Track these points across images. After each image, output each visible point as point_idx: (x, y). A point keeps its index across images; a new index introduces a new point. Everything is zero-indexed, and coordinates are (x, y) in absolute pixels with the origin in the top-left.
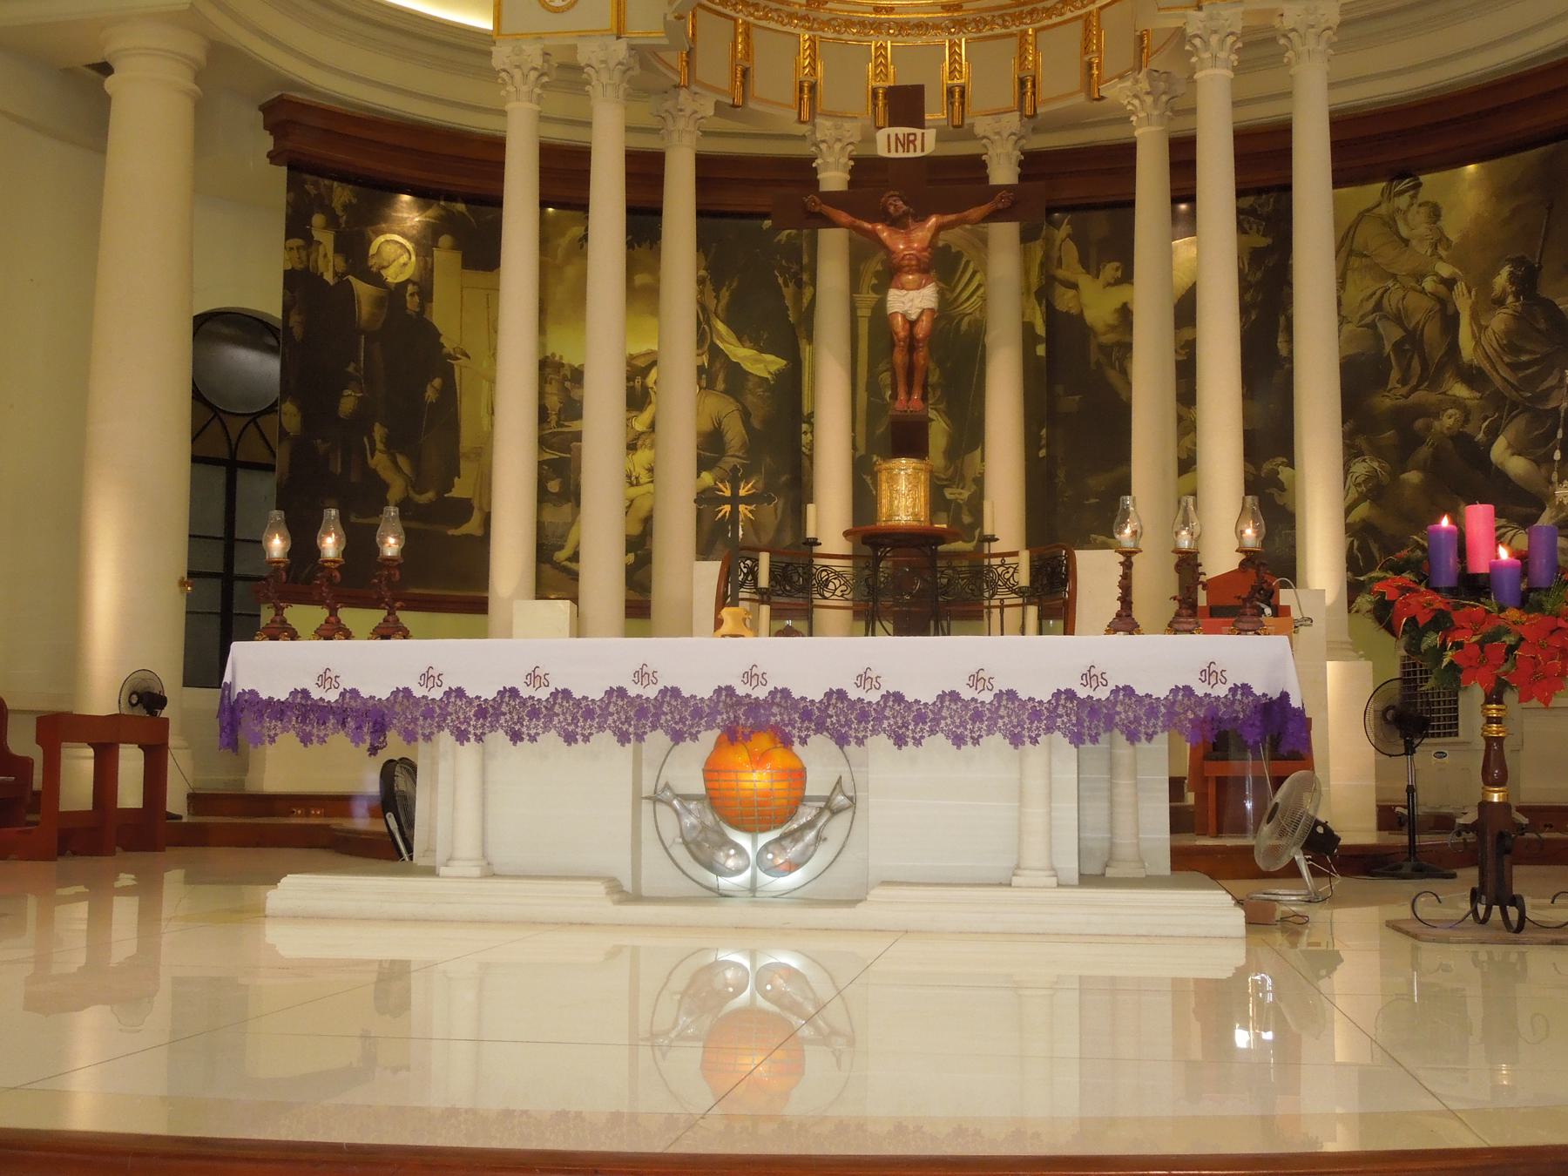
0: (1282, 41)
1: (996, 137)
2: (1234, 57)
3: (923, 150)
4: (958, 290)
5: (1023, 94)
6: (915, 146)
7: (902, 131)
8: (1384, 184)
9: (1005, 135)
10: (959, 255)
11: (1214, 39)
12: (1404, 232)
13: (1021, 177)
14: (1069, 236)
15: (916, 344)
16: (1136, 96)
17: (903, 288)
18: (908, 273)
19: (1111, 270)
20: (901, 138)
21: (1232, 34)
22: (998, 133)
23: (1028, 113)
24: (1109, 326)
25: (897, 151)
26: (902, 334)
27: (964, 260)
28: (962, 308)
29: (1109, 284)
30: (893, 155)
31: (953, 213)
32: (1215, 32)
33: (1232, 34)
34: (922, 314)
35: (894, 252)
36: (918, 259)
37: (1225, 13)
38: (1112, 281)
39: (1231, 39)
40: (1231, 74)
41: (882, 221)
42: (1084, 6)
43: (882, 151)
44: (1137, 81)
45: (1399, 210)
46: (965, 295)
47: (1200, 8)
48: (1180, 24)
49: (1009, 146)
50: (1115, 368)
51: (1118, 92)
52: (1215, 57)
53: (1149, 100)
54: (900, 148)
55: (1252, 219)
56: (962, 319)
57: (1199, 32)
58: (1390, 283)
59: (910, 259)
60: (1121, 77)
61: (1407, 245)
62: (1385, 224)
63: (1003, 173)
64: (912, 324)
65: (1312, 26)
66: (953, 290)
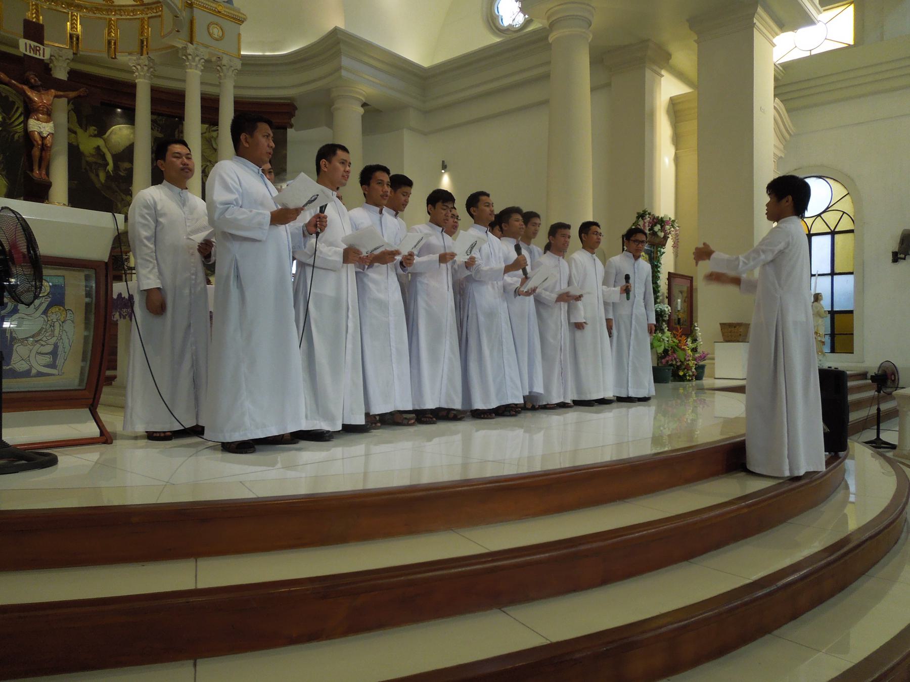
0: (219, 68)
1: (60, 58)
2: (202, 68)
3: (44, 56)
4: (13, 119)
5: (72, 42)
6: (39, 52)
7: (33, 44)
8: (207, 126)
9: (64, 58)
10: (13, 103)
11: (197, 59)
12: (214, 146)
13: (68, 78)
14: (72, 109)
15: (45, 148)
16: (139, 65)
17: (38, 120)
18: (43, 114)
19: (92, 130)
20: (33, 47)
21: (203, 58)
22: (61, 57)
23: (75, 52)
24: (90, 154)
25: (30, 52)
26: (40, 142)
27: (16, 106)
28: (16, 128)
29: (91, 136)
30: (28, 53)
31: (61, 91)
32: (197, 56)
33: (203, 58)
34: (48, 135)
35: (35, 102)
36: (48, 109)
37: (202, 50)
38: (93, 135)
39: (202, 61)
40: (200, 74)
41: (25, 85)
42: (109, 15)
43: (22, 49)
44: (140, 59)
45: (213, 137)
46: (17, 123)
47: (192, 43)
48: (180, 46)
49: (65, 65)
50: (93, 173)
51: (122, 58)
52: (196, 65)
53: (146, 68)
54: (32, 52)
55: (155, 125)
56: (14, 135)
57: (191, 53)
58: (208, 164)
59: (43, 108)
60: (130, 54)
61: (215, 151)
62: (207, 141)
63: (61, 74)
64: (43, 138)
65: (231, 67)
66: (10, 119)
